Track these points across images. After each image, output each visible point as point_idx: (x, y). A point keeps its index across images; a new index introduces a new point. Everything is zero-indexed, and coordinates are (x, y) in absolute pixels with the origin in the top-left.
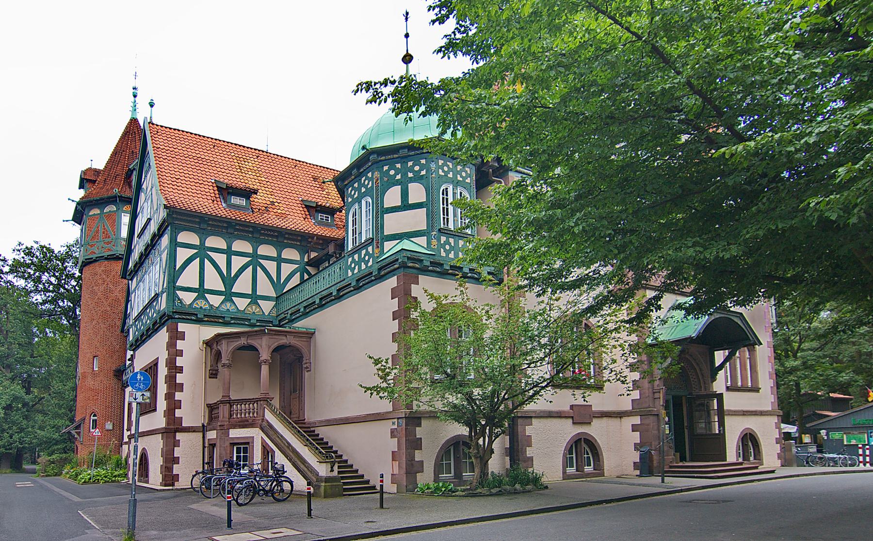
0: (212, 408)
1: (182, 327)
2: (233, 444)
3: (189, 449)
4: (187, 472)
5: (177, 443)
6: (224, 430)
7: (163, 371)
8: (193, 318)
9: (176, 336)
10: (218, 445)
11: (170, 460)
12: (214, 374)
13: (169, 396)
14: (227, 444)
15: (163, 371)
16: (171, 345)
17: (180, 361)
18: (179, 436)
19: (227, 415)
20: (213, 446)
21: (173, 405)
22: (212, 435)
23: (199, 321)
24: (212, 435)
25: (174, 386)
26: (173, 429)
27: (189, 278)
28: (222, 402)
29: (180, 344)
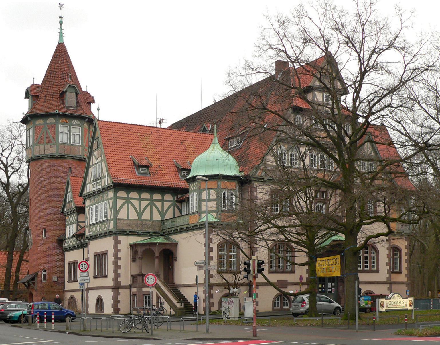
0: (134, 277)
1: (120, 238)
2: (144, 295)
3: (124, 295)
4: (124, 307)
5: (119, 294)
6: (140, 288)
7: (110, 259)
8: (125, 233)
9: (117, 242)
10: (137, 295)
11: (116, 301)
12: (134, 260)
13: (115, 271)
14: (142, 294)
15: (110, 259)
16: (115, 247)
17: (119, 255)
18: (120, 290)
19: (141, 281)
20: (135, 295)
21: (117, 276)
22: (134, 290)
23: (127, 235)
24: (134, 290)
25: (117, 267)
26: (117, 287)
27: (122, 215)
28: (139, 275)
29: (119, 247)
